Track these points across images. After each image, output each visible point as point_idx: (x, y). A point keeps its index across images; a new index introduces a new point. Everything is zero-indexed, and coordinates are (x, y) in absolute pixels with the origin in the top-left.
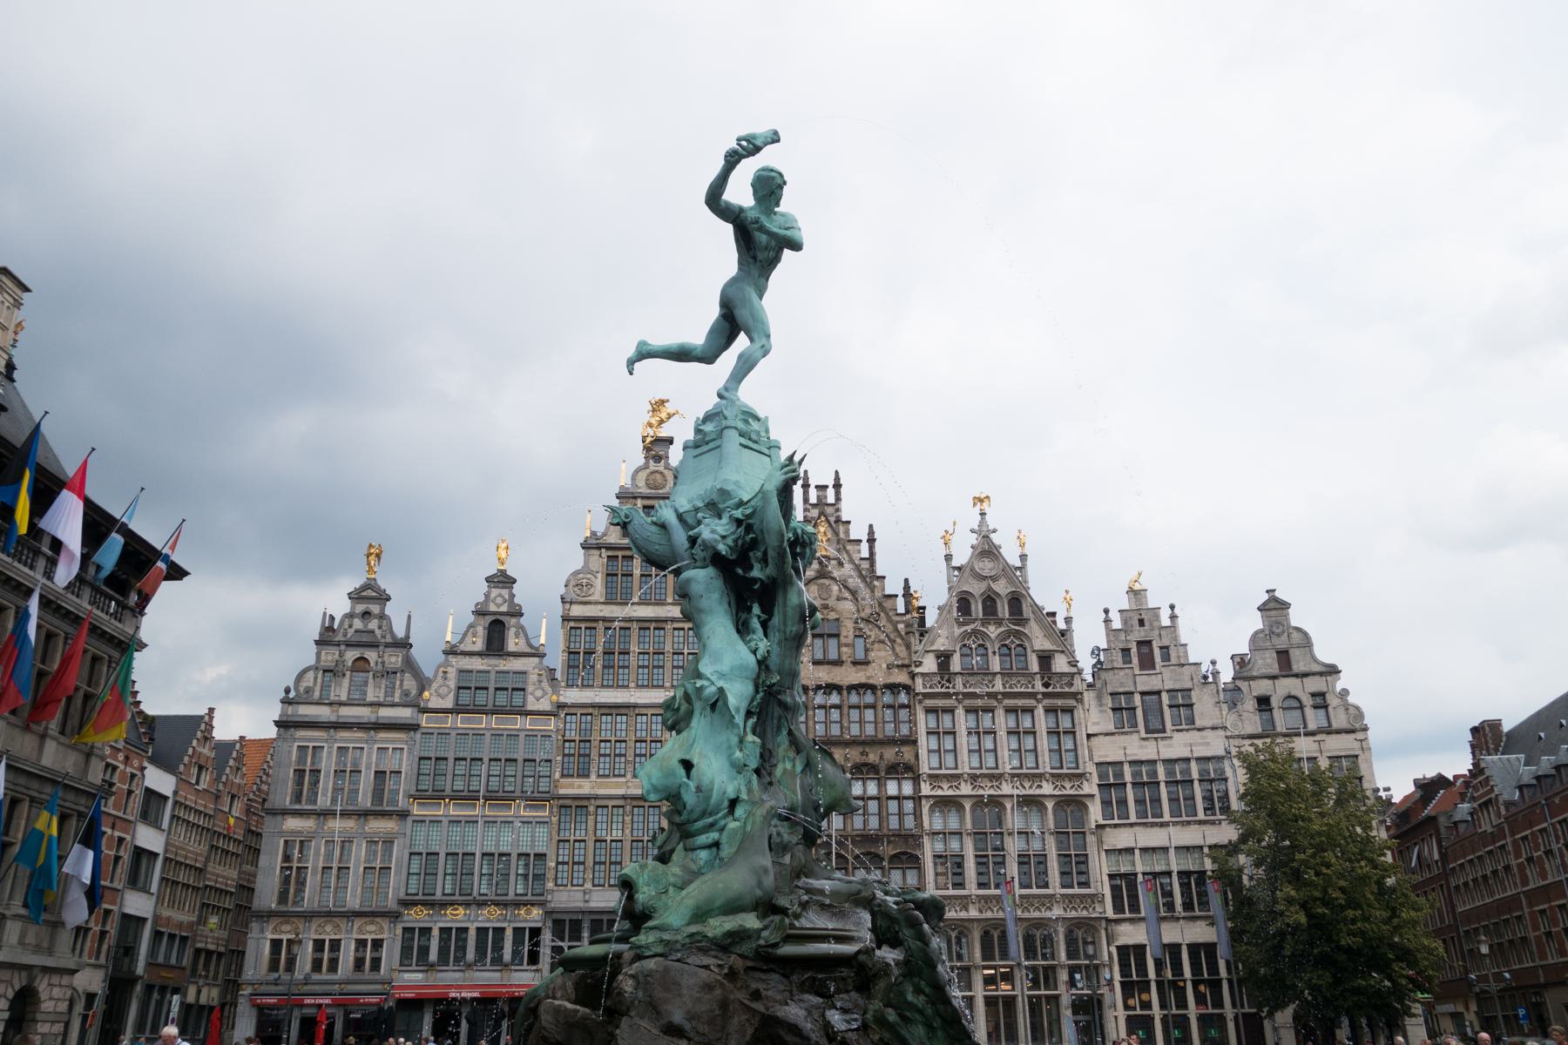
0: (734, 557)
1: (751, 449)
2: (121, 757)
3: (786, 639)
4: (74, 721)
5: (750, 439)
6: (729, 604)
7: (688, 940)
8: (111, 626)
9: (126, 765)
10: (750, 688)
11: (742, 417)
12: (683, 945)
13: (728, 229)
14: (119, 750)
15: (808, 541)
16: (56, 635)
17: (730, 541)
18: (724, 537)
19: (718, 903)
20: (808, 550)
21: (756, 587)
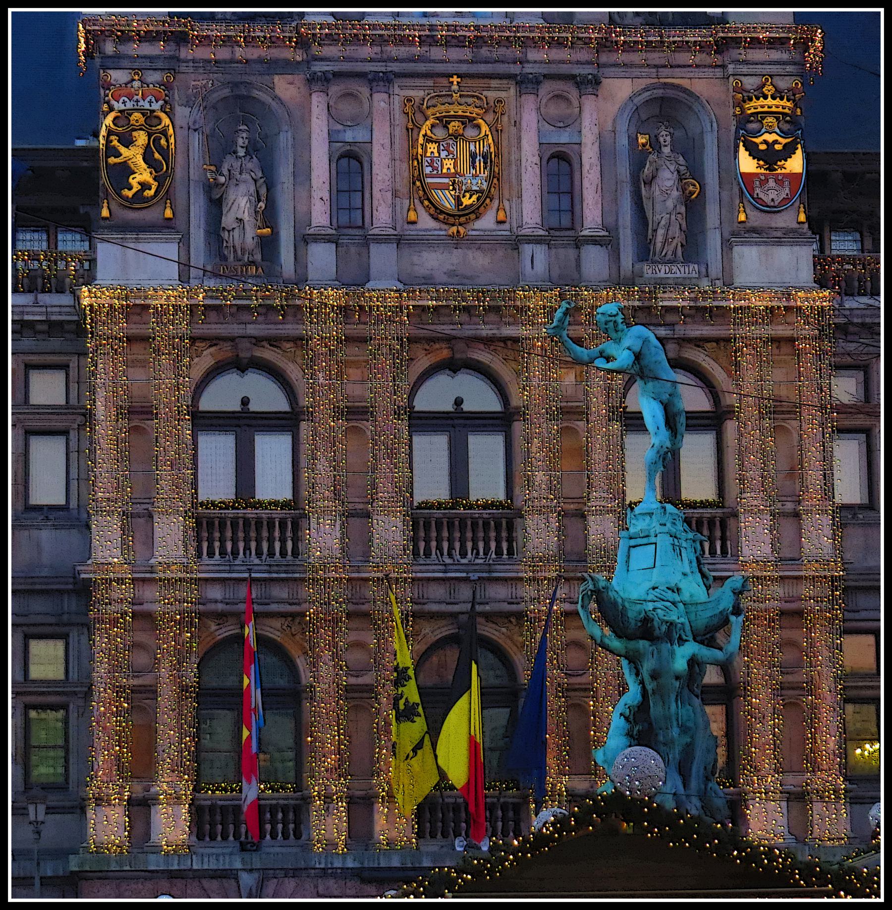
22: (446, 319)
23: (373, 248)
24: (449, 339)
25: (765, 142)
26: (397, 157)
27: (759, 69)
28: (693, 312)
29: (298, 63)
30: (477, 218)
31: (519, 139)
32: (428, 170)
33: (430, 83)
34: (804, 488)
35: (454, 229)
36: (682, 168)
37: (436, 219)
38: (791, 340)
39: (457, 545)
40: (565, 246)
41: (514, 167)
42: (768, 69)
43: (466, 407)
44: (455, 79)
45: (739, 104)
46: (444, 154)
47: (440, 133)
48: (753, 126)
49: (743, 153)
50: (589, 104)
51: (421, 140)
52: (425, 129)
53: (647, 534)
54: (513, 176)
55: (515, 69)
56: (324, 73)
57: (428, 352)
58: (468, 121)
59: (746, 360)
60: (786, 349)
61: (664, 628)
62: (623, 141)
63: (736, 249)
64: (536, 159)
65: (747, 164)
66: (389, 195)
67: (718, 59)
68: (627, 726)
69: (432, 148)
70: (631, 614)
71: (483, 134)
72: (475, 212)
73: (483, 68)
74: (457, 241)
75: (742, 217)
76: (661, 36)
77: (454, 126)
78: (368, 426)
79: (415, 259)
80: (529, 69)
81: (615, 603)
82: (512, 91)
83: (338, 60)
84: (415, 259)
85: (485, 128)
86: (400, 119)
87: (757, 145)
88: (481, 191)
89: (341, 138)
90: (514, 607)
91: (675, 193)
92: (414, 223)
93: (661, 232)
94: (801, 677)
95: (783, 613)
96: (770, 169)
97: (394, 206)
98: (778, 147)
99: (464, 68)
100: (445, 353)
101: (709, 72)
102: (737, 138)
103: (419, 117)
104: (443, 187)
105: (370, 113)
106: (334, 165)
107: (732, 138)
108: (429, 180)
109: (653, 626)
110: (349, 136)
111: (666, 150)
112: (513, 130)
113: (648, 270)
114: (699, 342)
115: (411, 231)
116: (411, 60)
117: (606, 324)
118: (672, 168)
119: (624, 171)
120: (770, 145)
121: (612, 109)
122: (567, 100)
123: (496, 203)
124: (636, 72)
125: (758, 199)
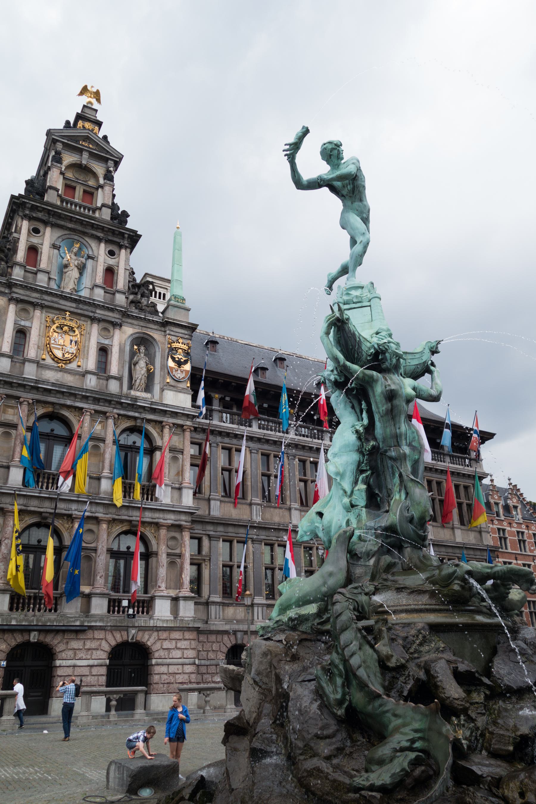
0: (343, 380)
1: (355, 308)
2: (524, 526)
3: (382, 416)
4: (466, 519)
5: (354, 303)
6: (353, 407)
7: (276, 625)
8: (468, 470)
9: (528, 530)
10: (355, 457)
11: (346, 292)
12: (273, 629)
13: (326, 190)
14: (521, 524)
15: (384, 349)
16: (442, 482)
17: (335, 372)
18: (332, 371)
19: (293, 600)
20: (387, 355)
21: (354, 393)
22: (53, 395)
23: (27, 364)
24: (53, 404)
25: (178, 358)
26: (41, 334)
27: (177, 334)
28: (149, 409)
29: (6, 293)
30: (70, 363)
31: (90, 339)
32: (52, 342)
33: (58, 312)
34: (183, 479)
35: (60, 365)
36: (148, 362)
37: (53, 360)
38: (182, 426)
39: (45, 484)
40: (103, 379)
41: (86, 348)
42: (180, 335)
43: (55, 432)
44: (68, 313)
45: (170, 343)
46: (60, 338)
47: (59, 331)
48: (174, 352)
49: (170, 359)
50: (117, 332)
51: (52, 330)
52: (54, 327)
53: (360, 300)
54: (86, 351)
55: (91, 314)
56: (17, 298)
57: (43, 407)
58: (72, 329)
59: (166, 431)
60: (179, 429)
61: (394, 361)
62: (128, 348)
63: (166, 392)
64: (96, 346)
65: (171, 363)
66: (36, 346)
67: (163, 329)
68: (358, 443)
69: (55, 334)
70: (363, 347)
71: (76, 334)
72: (70, 361)
73: (79, 311)
74: (62, 370)
75: (168, 380)
76: (145, 316)
77: (65, 328)
78: (13, 432)
79: (43, 373)
80: (96, 315)
81: (354, 334)
82: (89, 322)
83: (23, 295)
84: (43, 373)
85: (77, 332)
86: (43, 320)
87: (175, 358)
88: (73, 353)
89: (19, 323)
90: (67, 512)
91: (145, 369)
92: (44, 359)
93: (138, 381)
94: (177, 551)
95: (173, 525)
96: (179, 367)
97: (37, 352)
98: (182, 360)
99: (72, 310)
100: (50, 409)
101: (159, 333)
102: (168, 354)
103: (52, 323)
104: (59, 349)
105: (33, 317)
106: (15, 332)
107: (166, 354)
108: (52, 345)
109: (385, 359)
110: (23, 323)
111: (142, 355)
112: (88, 335)
113: (133, 393)
114: (149, 421)
115: (42, 362)
116: (52, 302)
117: (331, 152)
118: (144, 361)
119: (127, 358)
120: (180, 359)
121: (125, 337)
122: (109, 331)
123: (77, 359)
124: (135, 326)
125: (174, 376)
